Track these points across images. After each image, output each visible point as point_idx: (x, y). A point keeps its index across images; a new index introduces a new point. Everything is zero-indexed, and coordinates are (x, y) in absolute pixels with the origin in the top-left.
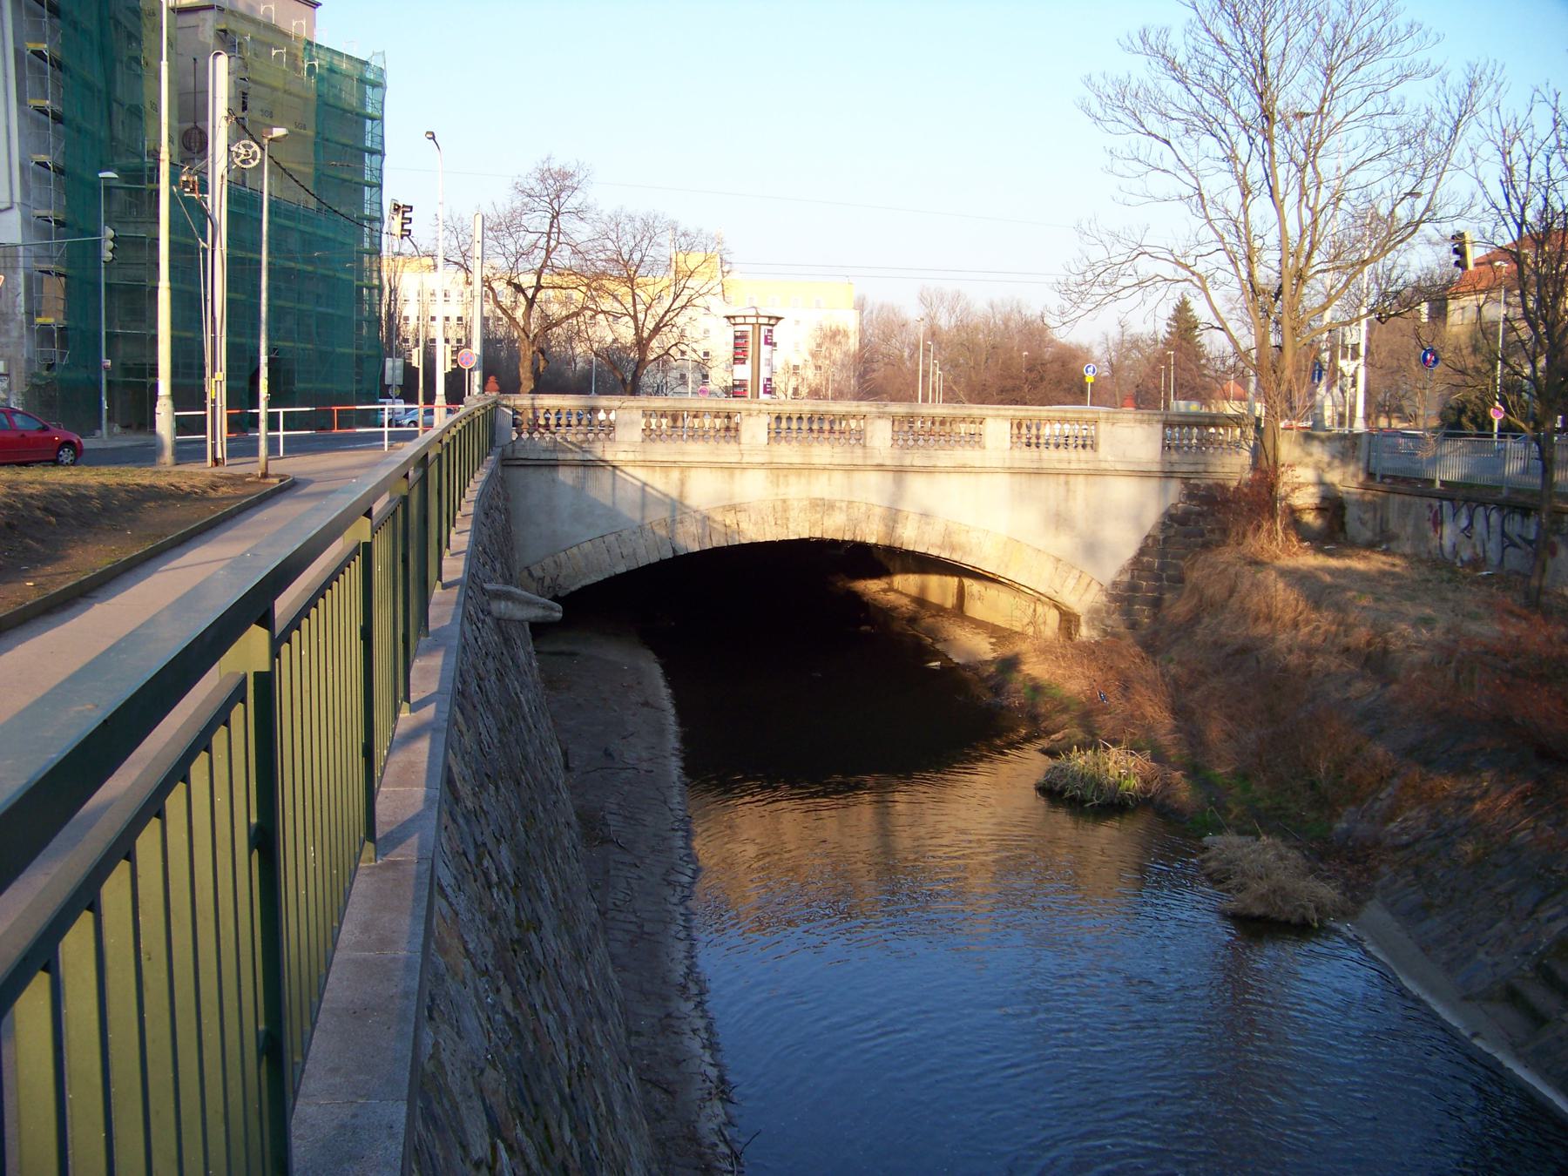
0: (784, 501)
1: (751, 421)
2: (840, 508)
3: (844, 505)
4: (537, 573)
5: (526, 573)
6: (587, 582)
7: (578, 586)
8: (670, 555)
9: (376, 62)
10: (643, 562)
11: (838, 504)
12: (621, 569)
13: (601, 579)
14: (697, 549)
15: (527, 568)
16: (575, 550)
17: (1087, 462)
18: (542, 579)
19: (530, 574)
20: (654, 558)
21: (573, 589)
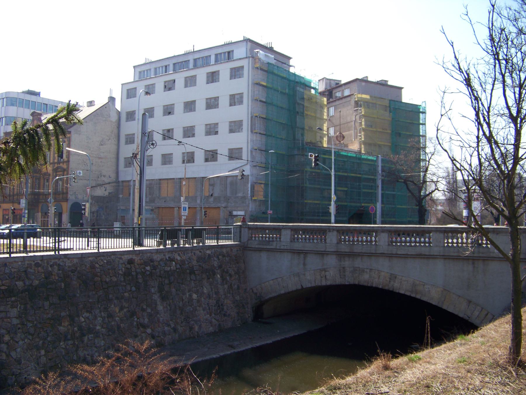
0: (344, 268)
1: (330, 234)
2: (367, 272)
3: (368, 271)
4: (255, 291)
5: (251, 291)
6: (271, 296)
7: (268, 297)
8: (300, 287)
9: (423, 105)
10: (290, 290)
11: (365, 270)
12: (283, 292)
13: (276, 295)
14: (310, 286)
15: (252, 289)
16: (267, 283)
17: (483, 253)
18: (256, 294)
19: (253, 291)
20: (294, 288)
21: (266, 298)
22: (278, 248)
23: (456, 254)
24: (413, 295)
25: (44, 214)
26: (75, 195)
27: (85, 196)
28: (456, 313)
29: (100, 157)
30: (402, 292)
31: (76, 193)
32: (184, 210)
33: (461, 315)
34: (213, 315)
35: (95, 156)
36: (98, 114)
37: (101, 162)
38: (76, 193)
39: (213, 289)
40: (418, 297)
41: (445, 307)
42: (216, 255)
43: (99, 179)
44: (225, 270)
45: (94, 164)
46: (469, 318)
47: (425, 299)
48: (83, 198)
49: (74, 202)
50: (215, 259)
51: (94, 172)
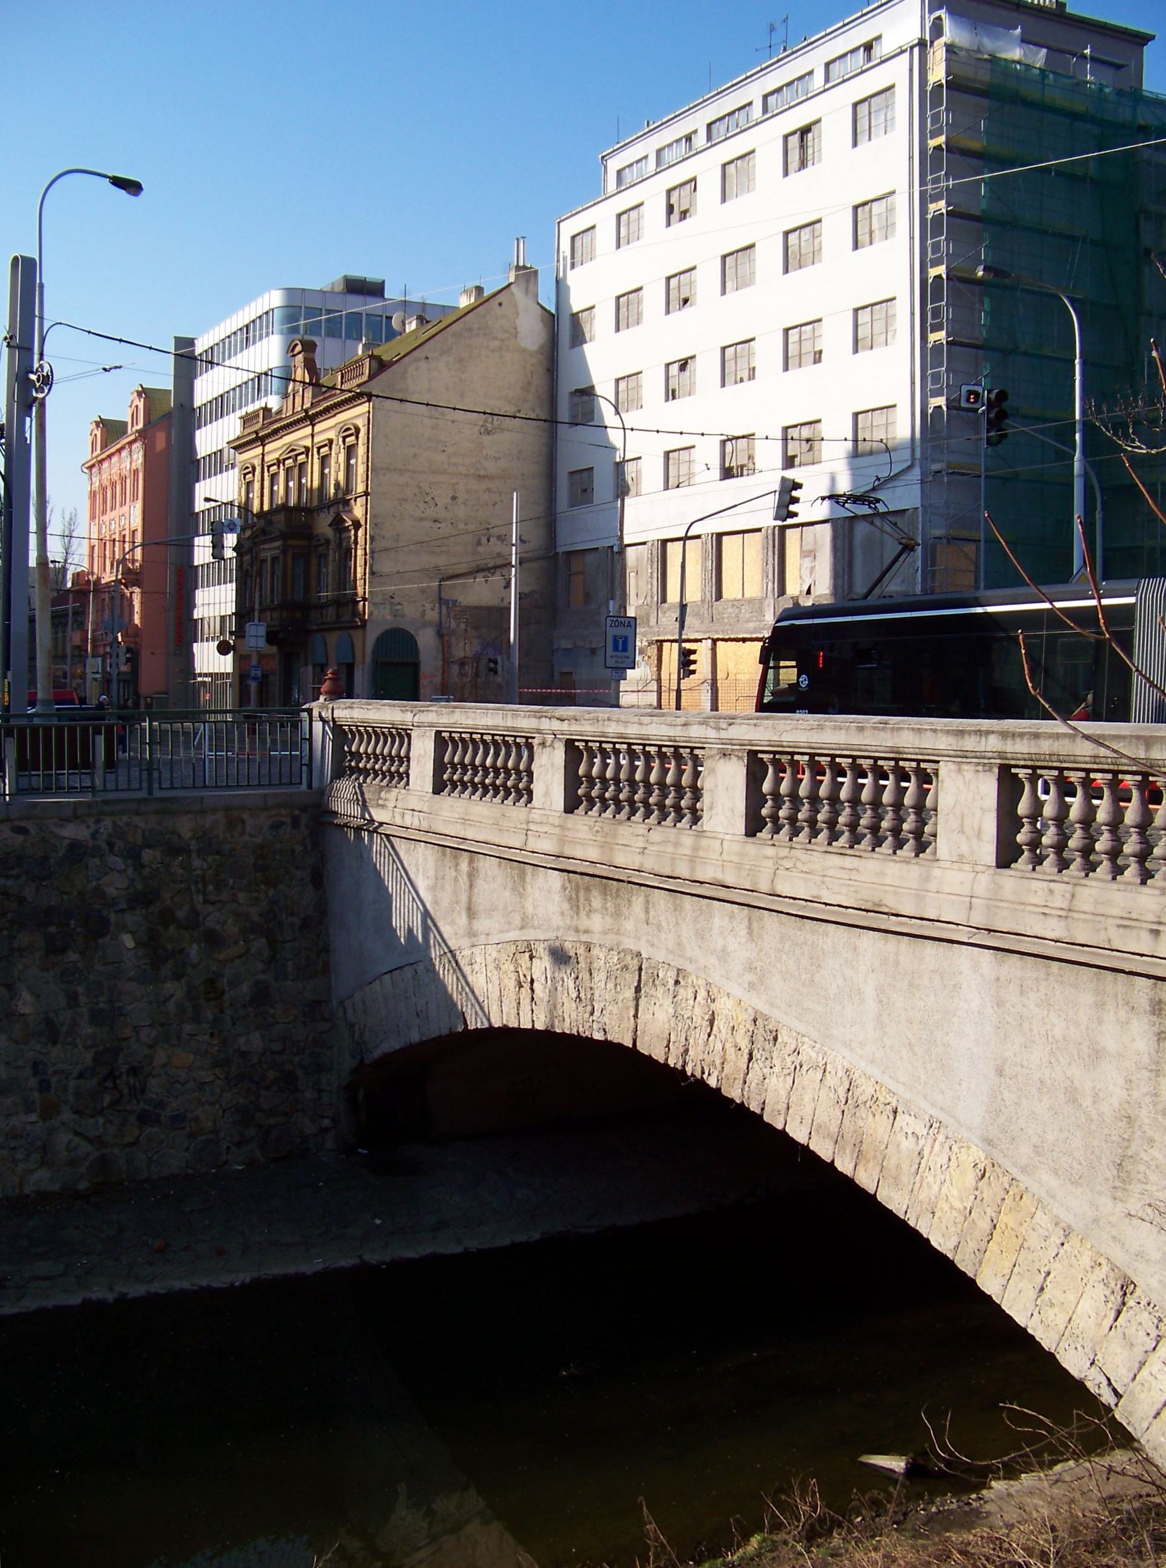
18: (353, 1026)
22: (398, 821)
23: (1053, 928)
24: (844, 1165)
25: (318, 669)
26: (392, 604)
27: (428, 606)
28: (1047, 1342)
29: (482, 473)
30: (798, 1134)
31: (396, 600)
32: (616, 649)
33: (1073, 1363)
34: (67, 1115)
35: (462, 470)
36: (470, 330)
37: (489, 490)
38: (396, 600)
39: (83, 1000)
40: (866, 1179)
41: (989, 1284)
42: (119, 844)
43: (481, 549)
44: (180, 914)
45: (460, 501)
46: (1118, 1395)
47: (894, 1200)
48: (423, 614)
49: (387, 627)
50: (117, 862)
51: (461, 526)
